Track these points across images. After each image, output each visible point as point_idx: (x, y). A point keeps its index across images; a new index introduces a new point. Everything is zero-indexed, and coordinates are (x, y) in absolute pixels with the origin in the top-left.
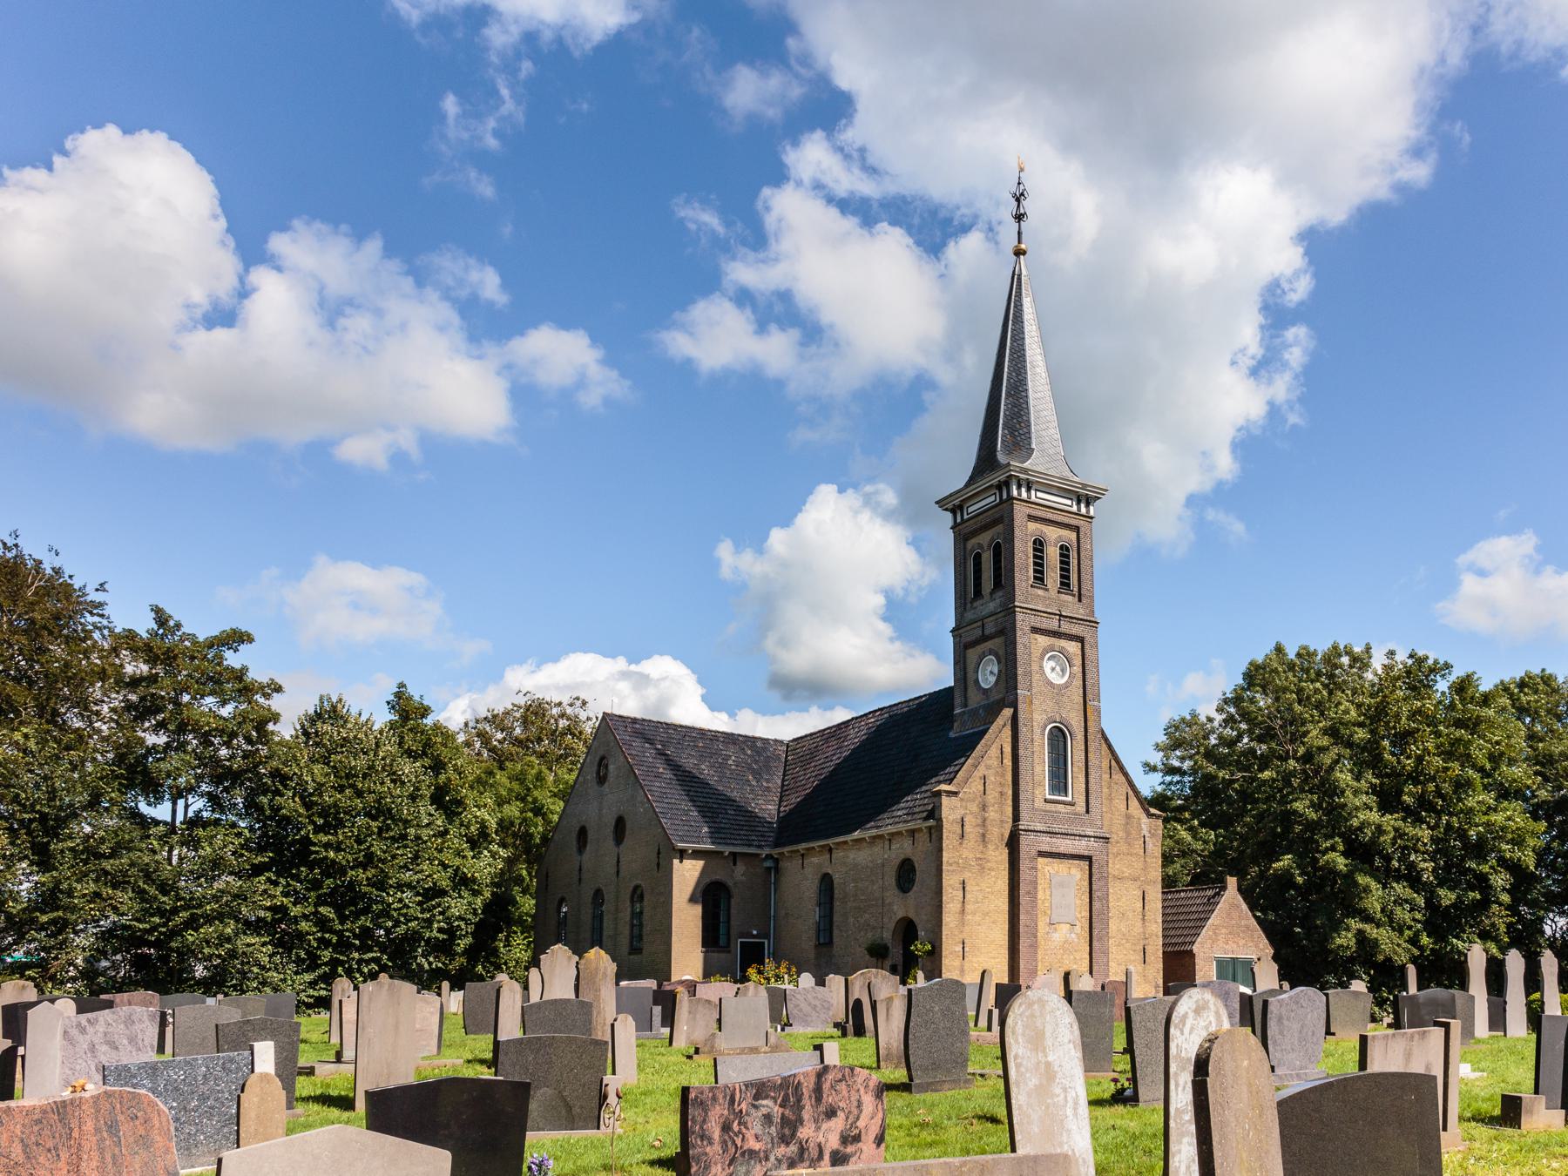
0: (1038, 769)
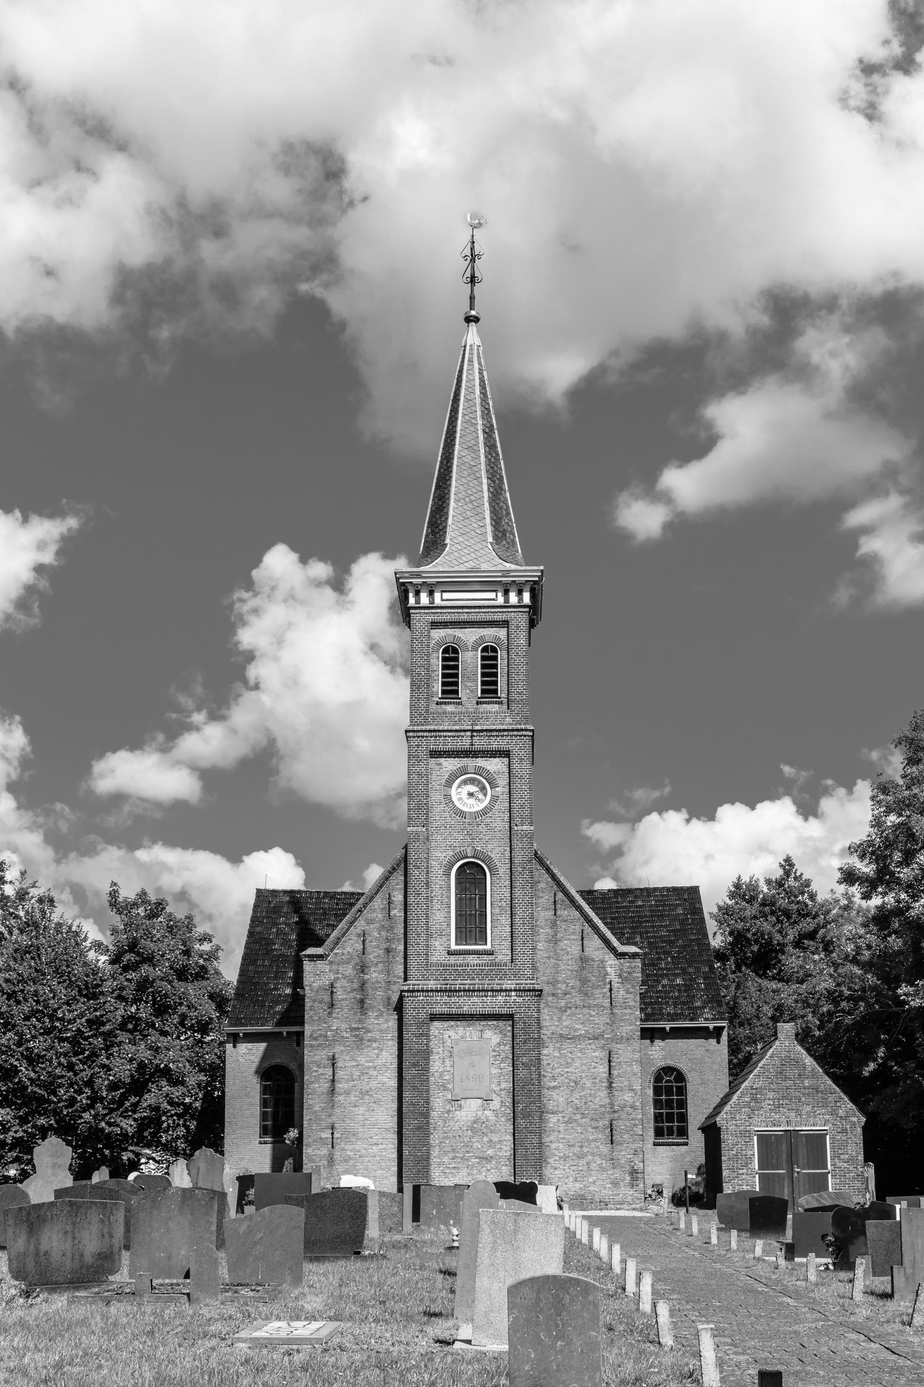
0: (438, 916)
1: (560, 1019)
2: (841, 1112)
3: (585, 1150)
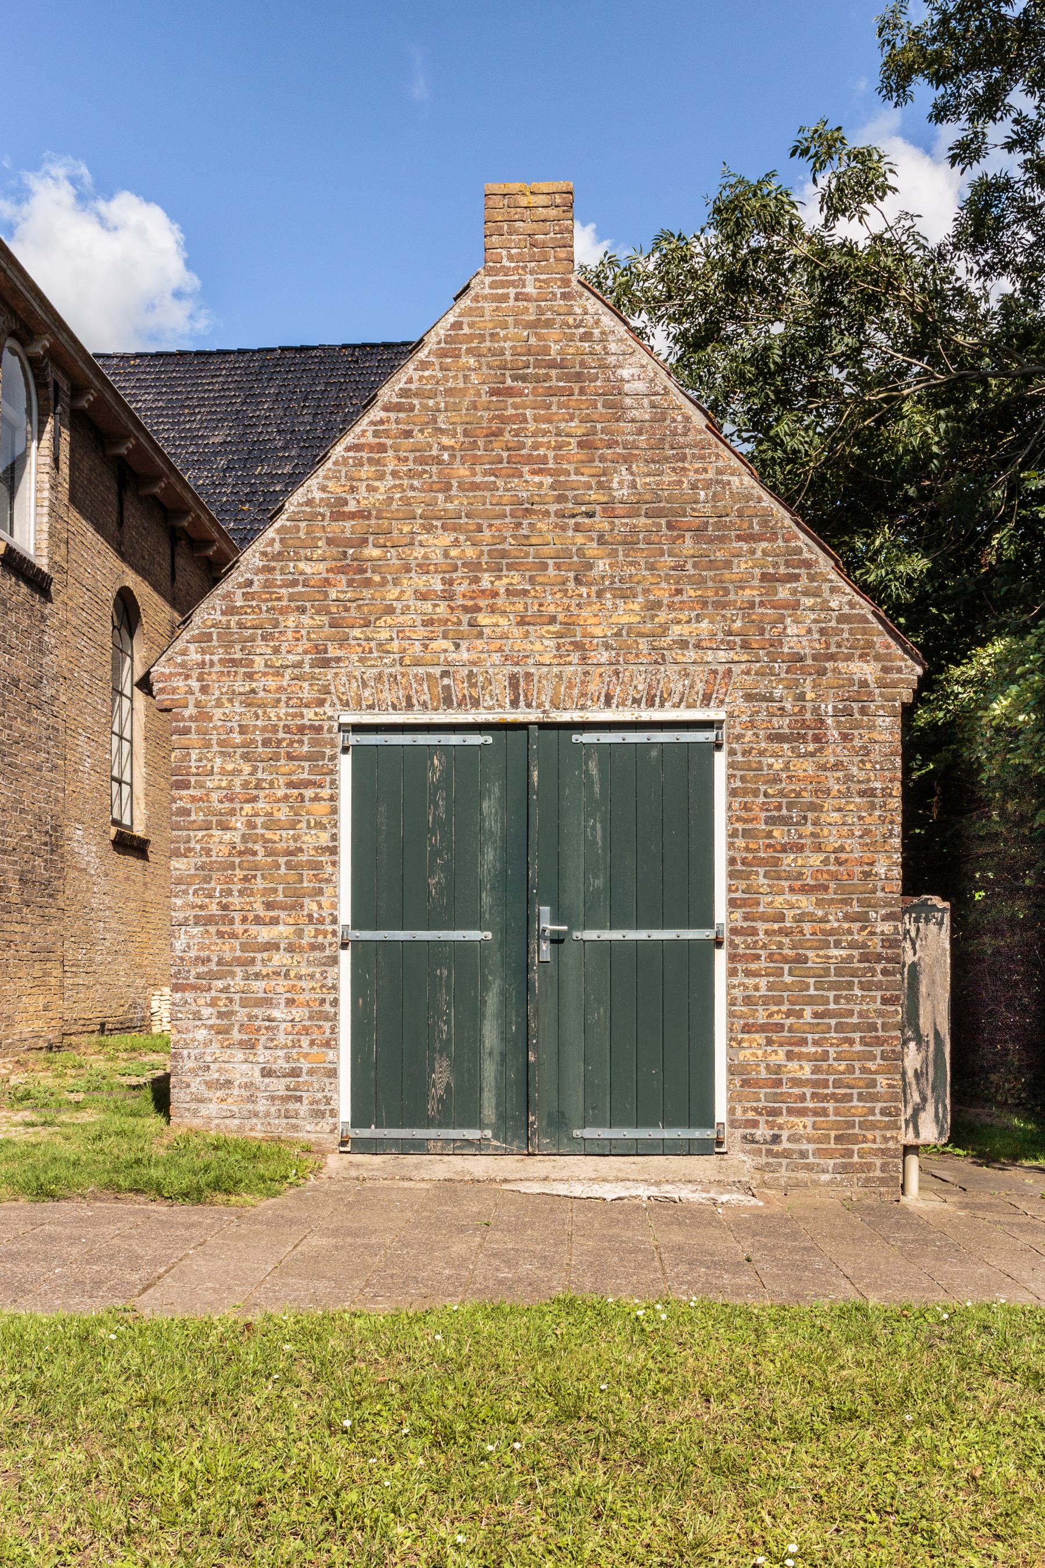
2: (796, 636)
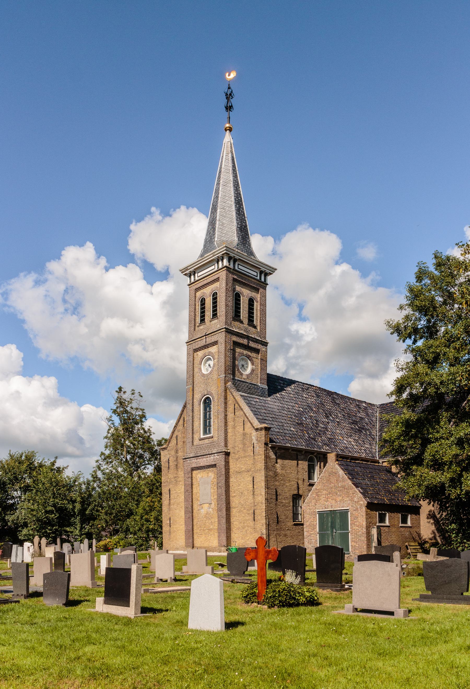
1: (236, 464)
2: (356, 499)
3: (245, 524)
